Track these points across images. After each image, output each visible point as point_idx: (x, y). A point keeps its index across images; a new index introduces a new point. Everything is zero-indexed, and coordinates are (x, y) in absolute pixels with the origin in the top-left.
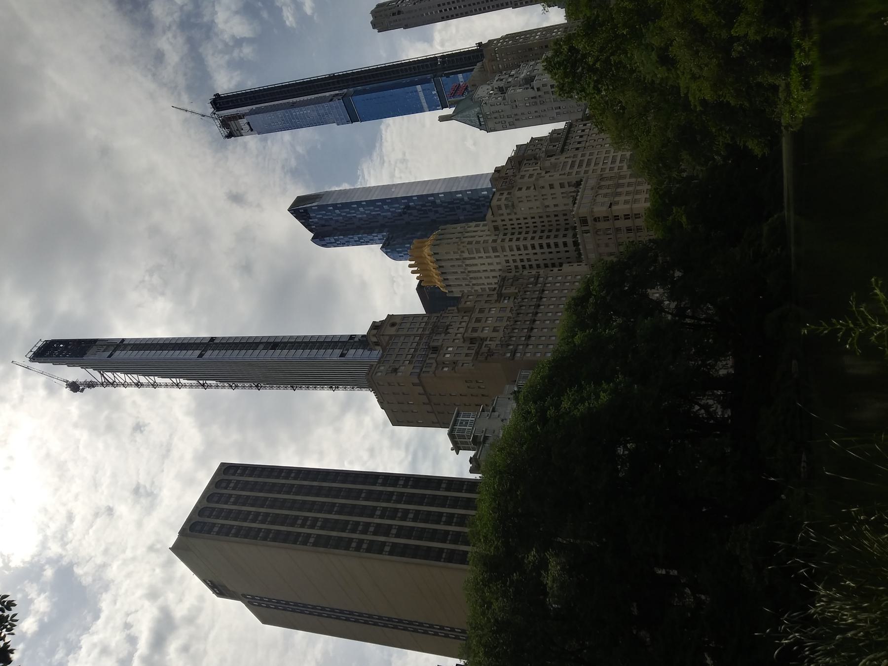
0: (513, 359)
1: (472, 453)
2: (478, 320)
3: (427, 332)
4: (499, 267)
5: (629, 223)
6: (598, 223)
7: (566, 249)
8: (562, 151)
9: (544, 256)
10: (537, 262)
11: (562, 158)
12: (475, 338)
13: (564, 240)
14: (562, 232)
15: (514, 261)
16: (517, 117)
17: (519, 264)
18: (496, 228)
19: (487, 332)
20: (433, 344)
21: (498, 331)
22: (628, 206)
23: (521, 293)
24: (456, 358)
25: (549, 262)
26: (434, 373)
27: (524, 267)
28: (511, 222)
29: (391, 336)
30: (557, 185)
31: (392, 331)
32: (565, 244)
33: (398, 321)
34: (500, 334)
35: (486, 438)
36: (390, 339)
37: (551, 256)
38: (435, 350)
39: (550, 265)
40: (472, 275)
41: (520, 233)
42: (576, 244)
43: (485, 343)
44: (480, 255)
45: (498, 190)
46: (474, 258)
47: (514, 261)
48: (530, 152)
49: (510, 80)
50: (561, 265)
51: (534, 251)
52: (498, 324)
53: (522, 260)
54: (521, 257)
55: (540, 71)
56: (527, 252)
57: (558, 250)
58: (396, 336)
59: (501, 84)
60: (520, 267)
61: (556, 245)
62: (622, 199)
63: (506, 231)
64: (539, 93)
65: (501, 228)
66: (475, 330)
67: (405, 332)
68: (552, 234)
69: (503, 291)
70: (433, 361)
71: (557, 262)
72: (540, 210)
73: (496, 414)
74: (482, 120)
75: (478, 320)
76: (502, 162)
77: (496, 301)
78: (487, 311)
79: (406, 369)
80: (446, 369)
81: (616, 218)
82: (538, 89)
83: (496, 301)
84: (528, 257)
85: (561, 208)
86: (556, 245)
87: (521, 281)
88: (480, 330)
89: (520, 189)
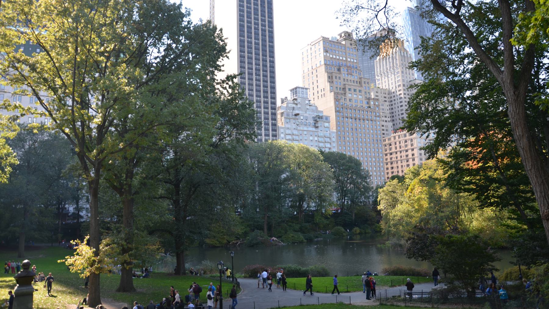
1: (289, 98)
2: (355, 90)
4: (391, 88)
6: (410, 141)
12: (345, 91)
15: (394, 96)
17: (393, 99)
19: (349, 95)
21: (350, 101)
25: (394, 114)
27: (391, 101)
34: (348, 102)
35: (297, 104)
37: (397, 115)
38: (339, 70)
52: (353, 100)
53: (395, 100)
60: (391, 99)
66: (350, 89)
67: (347, 52)
73: (308, 107)
75: (355, 90)
77: (366, 97)
78: (360, 94)
83: (366, 97)
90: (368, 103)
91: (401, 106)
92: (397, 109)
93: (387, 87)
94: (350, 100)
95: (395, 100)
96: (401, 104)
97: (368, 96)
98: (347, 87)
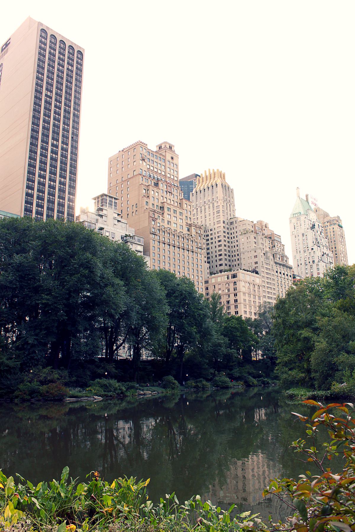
0: (151, 233)
2: (175, 211)
3: (167, 180)
5: (232, 302)
6: (233, 284)
7: (218, 266)
8: (276, 263)
9: (214, 252)
10: (210, 248)
11: (272, 263)
13: (224, 265)
14: (228, 263)
15: (211, 234)
16: (297, 236)
18: (232, 223)
19: (167, 217)
20: (160, 183)
21: (168, 224)
22: (242, 301)
23: (192, 239)
24: (151, 197)
25: (210, 256)
26: (142, 184)
27: (208, 240)
28: (235, 233)
29: (165, 156)
30: (256, 260)
31: (168, 158)
32: (221, 265)
33: (175, 161)
34: (166, 225)
35: (101, 216)
36: (163, 156)
38: (156, 185)
39: (209, 256)
40: (203, 208)
41: (228, 238)
42: (221, 271)
43: (161, 216)
44: (215, 213)
45: (255, 225)
46: (213, 210)
47: (211, 234)
48: (276, 244)
49: (319, 233)
50: (209, 262)
51: (217, 246)
53: (212, 239)
54: (214, 238)
55: (322, 250)
56: (217, 242)
57: (218, 260)
58: (165, 161)
59: (316, 226)
60: (208, 238)
61: (220, 260)
62: (247, 298)
63: (230, 229)
64: (310, 249)
65: (232, 227)
66: (169, 209)
67: (168, 165)
68: (227, 257)
69: (193, 227)
70: (150, 183)
71: (210, 260)
72: (242, 250)
73: (116, 222)
74: (297, 215)
75: (175, 211)
76: (271, 227)
77: (187, 223)
79: (144, 166)
80: (144, 191)
81: (236, 295)
82: (312, 249)
83: (187, 223)
84: (214, 243)
85: (243, 262)
86: (220, 260)
87: (199, 238)
88: (169, 213)
89: (255, 238)
90: (188, 230)
91: (220, 246)
92: (214, 250)
93: (203, 223)
94: (168, 222)
95: (212, 239)
96: (220, 243)
97: (189, 222)
98: (166, 206)
